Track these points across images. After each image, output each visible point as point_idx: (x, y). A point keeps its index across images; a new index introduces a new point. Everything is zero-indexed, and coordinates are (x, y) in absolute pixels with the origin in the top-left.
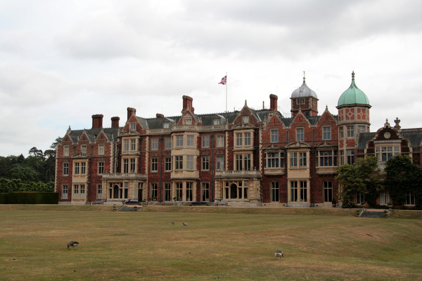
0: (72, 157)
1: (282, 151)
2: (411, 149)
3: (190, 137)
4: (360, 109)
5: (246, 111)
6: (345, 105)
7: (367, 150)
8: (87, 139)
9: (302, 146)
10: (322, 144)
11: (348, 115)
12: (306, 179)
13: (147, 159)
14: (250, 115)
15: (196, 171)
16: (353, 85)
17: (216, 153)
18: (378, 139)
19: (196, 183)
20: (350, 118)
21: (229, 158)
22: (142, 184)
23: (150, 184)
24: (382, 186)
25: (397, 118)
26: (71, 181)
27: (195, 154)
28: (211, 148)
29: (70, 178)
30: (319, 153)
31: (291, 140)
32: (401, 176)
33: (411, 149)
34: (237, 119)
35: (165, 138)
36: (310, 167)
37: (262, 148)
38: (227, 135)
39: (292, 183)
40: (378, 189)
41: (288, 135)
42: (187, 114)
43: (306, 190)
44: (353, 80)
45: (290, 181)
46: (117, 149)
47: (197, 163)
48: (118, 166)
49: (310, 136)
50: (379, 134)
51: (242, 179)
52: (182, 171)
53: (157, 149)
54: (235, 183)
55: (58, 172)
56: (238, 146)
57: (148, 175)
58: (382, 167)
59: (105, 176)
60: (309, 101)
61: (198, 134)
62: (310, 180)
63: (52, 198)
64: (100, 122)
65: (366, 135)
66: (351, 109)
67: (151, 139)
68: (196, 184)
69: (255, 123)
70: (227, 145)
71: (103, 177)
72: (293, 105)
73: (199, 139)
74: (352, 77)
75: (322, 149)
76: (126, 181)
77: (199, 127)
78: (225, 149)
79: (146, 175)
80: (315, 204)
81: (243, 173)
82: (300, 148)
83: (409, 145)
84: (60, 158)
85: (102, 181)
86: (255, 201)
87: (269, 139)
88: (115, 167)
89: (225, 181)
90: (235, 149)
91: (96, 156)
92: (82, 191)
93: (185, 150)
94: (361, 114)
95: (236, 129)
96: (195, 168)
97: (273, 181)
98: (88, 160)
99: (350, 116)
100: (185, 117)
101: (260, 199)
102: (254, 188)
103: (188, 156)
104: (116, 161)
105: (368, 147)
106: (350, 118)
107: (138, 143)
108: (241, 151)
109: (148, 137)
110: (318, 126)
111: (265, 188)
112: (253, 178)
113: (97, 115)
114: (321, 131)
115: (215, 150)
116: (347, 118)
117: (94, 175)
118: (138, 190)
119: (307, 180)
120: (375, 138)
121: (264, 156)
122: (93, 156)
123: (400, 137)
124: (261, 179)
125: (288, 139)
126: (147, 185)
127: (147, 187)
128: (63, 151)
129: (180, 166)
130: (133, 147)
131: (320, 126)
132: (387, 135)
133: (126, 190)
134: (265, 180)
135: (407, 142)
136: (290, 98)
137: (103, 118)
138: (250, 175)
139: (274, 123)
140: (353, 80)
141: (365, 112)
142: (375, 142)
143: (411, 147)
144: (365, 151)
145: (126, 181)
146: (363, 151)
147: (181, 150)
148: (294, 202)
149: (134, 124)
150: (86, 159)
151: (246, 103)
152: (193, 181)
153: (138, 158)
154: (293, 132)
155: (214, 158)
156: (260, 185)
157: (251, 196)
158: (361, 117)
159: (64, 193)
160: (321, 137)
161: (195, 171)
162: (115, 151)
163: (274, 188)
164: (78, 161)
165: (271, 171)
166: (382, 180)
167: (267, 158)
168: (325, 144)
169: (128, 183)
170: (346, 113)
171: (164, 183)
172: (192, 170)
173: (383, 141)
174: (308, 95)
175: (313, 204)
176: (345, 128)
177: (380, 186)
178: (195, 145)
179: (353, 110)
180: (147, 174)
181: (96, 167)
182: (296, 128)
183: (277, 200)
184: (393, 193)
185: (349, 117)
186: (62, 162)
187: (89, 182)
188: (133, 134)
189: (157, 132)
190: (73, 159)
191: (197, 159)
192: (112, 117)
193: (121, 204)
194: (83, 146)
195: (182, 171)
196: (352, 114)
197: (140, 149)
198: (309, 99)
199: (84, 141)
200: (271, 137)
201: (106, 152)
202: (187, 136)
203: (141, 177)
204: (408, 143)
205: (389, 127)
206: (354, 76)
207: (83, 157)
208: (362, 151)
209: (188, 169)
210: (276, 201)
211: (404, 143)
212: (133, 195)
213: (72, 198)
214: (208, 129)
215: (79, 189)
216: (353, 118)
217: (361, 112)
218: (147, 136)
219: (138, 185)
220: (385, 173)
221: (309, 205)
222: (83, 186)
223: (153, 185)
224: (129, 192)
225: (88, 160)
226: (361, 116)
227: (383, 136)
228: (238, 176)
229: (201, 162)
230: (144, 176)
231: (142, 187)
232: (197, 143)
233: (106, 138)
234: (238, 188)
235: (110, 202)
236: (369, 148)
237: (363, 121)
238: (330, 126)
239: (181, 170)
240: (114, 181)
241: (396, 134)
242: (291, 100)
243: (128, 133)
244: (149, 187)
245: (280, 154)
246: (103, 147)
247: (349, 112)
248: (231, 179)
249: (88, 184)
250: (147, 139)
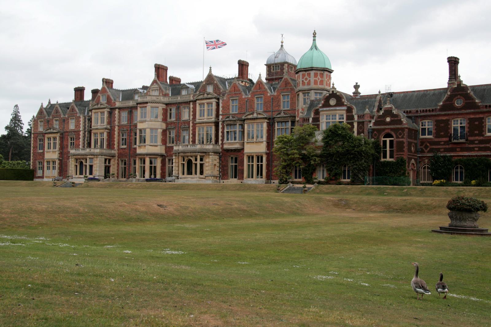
0: (44, 132)
1: (241, 122)
2: (356, 118)
3: (155, 108)
4: (318, 73)
5: (210, 79)
6: (301, 69)
7: (313, 118)
8: (59, 113)
9: (260, 116)
10: (280, 114)
11: (304, 81)
12: (262, 153)
13: (116, 133)
14: (214, 83)
15: (161, 145)
16: (314, 47)
17: (181, 126)
18: (324, 106)
19: (161, 158)
20: (306, 84)
21: (193, 131)
22: (110, 160)
23: (119, 160)
24: (317, 159)
25: (357, 83)
26: (44, 157)
27: (160, 127)
28: (176, 120)
29: (43, 153)
30: (276, 124)
31: (250, 110)
32: (337, 147)
33: (356, 118)
34: (201, 88)
35: (134, 111)
36: (267, 140)
37: (222, 119)
38: (191, 106)
39: (249, 157)
40: (312, 163)
41: (247, 105)
42: (155, 84)
43: (262, 165)
44: (314, 40)
45: (247, 156)
46: (88, 123)
47: (162, 137)
48: (89, 141)
49: (269, 105)
50: (324, 100)
51: (197, 154)
52: (145, 146)
53: (126, 123)
54: (191, 158)
55: (34, 148)
56: (201, 118)
57: (118, 150)
58: (319, 137)
59: (72, 151)
60: (284, 67)
61: (165, 106)
62: (267, 154)
63: (28, 175)
64: (81, 95)
65: (316, 102)
66: (308, 74)
67: (121, 112)
68: (161, 160)
69: (218, 92)
70: (191, 117)
71: (71, 152)
72: (268, 73)
73: (165, 112)
74: (313, 37)
75: (280, 120)
76: (90, 157)
77: (165, 98)
78: (190, 121)
79: (115, 150)
80: (272, 181)
81: (198, 147)
82: (257, 118)
83: (354, 112)
84: (35, 132)
85: (69, 156)
86: (210, 178)
87: (229, 109)
88: (86, 142)
89: (182, 156)
90: (197, 121)
91: (68, 131)
92: (54, 168)
93: (150, 123)
94: (319, 79)
95: (198, 99)
96: (159, 142)
97: (232, 156)
98: (59, 134)
99: (306, 82)
100: (153, 87)
101: (219, 175)
102: (211, 164)
103: (152, 129)
104: (87, 135)
105: (314, 115)
106: (306, 84)
107: (108, 116)
108: (204, 123)
110: (277, 94)
111: (224, 164)
112: (209, 152)
113: (79, 88)
114: (280, 99)
115: (180, 123)
116: (303, 83)
117: (65, 151)
118: (104, 166)
119: (263, 154)
120: (321, 105)
121: (223, 128)
122: (65, 131)
123: (345, 104)
124: (220, 153)
125: (247, 110)
126: (116, 162)
127: (116, 163)
128: (38, 125)
129: (143, 140)
130: (102, 122)
131: (279, 94)
132: (333, 102)
133: (91, 167)
134: (224, 155)
135: (352, 109)
136: (265, 65)
137: (85, 91)
138: (206, 149)
139: (235, 92)
140: (314, 40)
141: (323, 76)
142: (320, 109)
143: (356, 114)
144: (311, 120)
145: (90, 157)
146: (309, 120)
147: (144, 123)
148: (251, 179)
149: (105, 96)
150: (57, 134)
151: (210, 70)
152: (157, 157)
153: (107, 132)
154: (253, 101)
155: (179, 131)
156: (218, 161)
157: (207, 172)
158: (319, 83)
159: (39, 169)
160: (280, 106)
161: (159, 145)
162: (85, 125)
163: (231, 163)
164: (50, 135)
165: (230, 145)
166: (319, 152)
167: (226, 130)
168: (282, 114)
169: (93, 158)
170: (303, 78)
171: (132, 160)
172: (155, 144)
173: (328, 109)
174: (283, 61)
175: (269, 181)
176: (301, 94)
177: (315, 159)
178: (160, 118)
179: (309, 75)
180: (117, 150)
181: (68, 142)
182: (255, 96)
183: (235, 177)
184: (329, 167)
185: (305, 83)
186: (37, 137)
187: (61, 158)
188: (102, 106)
189: (127, 104)
190: (45, 133)
191: (162, 132)
192: (92, 89)
193: (82, 181)
194: (56, 120)
195: (145, 146)
196: (309, 79)
197: (109, 123)
198: (284, 65)
199: (56, 115)
200: (231, 107)
201: (76, 126)
202: (151, 107)
203: (107, 152)
204: (354, 110)
205: (335, 92)
206: (315, 37)
207: (55, 131)
208: (307, 121)
209: (152, 144)
210: (235, 178)
211: (349, 110)
212: (98, 171)
213: (45, 175)
214: (175, 100)
215: (51, 165)
216: (309, 84)
217: (319, 77)
218: (117, 108)
219: (104, 161)
220: (322, 144)
221: (264, 182)
222: (54, 162)
223: (122, 161)
224: (94, 169)
225: (59, 134)
226: (319, 81)
227: (329, 102)
228: (193, 151)
229: (166, 136)
230: (113, 152)
231: (109, 163)
232: (163, 115)
233: (76, 112)
234: (194, 163)
235: (75, 179)
236: (315, 117)
237: (321, 86)
238: (289, 93)
239: (144, 144)
240: (79, 157)
241: (341, 101)
242: (266, 66)
243: (98, 105)
244: (118, 164)
245: (238, 125)
246: (74, 121)
247: (305, 77)
248: (187, 154)
249: (59, 160)
250: (117, 111)
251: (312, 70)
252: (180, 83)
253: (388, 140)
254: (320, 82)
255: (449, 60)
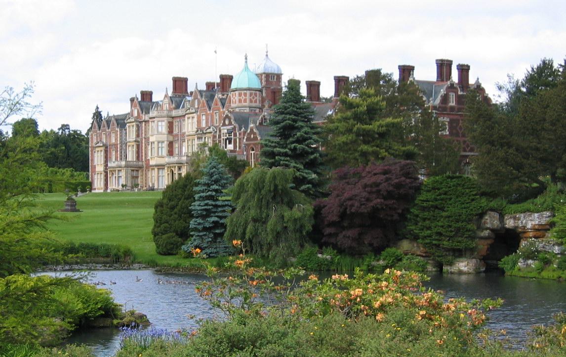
4: (241, 93)
18: (223, 126)
44: (246, 62)
109: (144, 123)
132: (227, 122)
140: (246, 62)
145: (119, 169)
169: (121, 170)
197: (138, 136)
230: (140, 163)
240: (112, 169)
251: (236, 90)
252: (36, 133)
253: (253, 152)
254: (244, 100)
255: (307, 83)
